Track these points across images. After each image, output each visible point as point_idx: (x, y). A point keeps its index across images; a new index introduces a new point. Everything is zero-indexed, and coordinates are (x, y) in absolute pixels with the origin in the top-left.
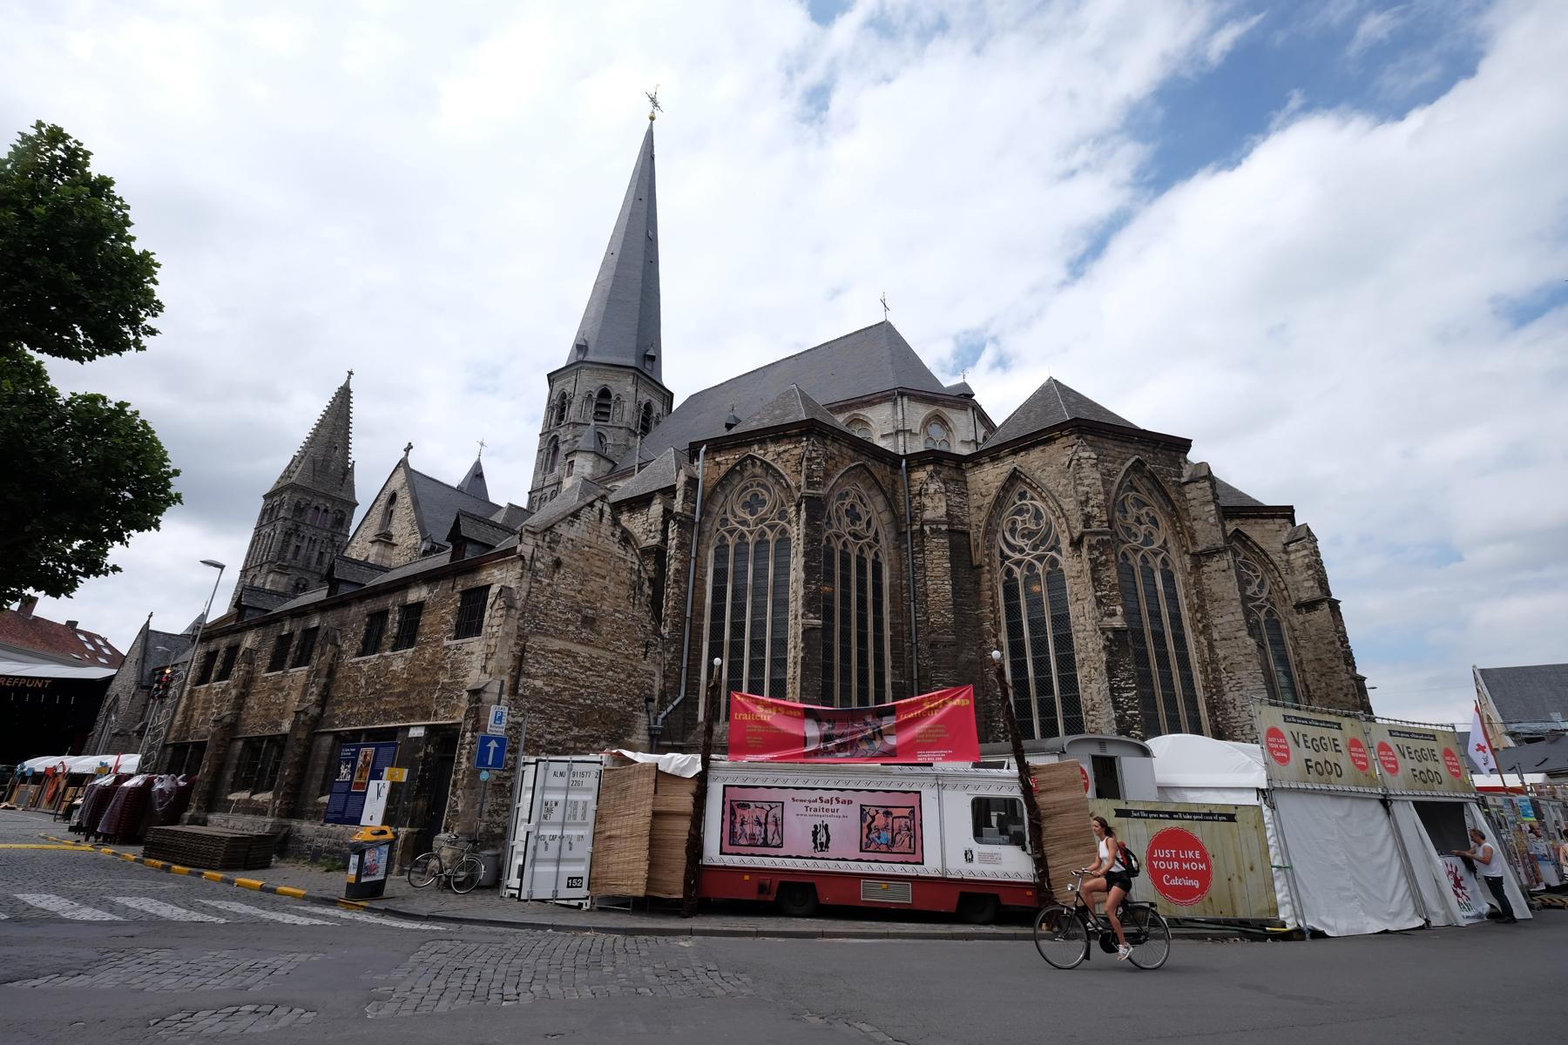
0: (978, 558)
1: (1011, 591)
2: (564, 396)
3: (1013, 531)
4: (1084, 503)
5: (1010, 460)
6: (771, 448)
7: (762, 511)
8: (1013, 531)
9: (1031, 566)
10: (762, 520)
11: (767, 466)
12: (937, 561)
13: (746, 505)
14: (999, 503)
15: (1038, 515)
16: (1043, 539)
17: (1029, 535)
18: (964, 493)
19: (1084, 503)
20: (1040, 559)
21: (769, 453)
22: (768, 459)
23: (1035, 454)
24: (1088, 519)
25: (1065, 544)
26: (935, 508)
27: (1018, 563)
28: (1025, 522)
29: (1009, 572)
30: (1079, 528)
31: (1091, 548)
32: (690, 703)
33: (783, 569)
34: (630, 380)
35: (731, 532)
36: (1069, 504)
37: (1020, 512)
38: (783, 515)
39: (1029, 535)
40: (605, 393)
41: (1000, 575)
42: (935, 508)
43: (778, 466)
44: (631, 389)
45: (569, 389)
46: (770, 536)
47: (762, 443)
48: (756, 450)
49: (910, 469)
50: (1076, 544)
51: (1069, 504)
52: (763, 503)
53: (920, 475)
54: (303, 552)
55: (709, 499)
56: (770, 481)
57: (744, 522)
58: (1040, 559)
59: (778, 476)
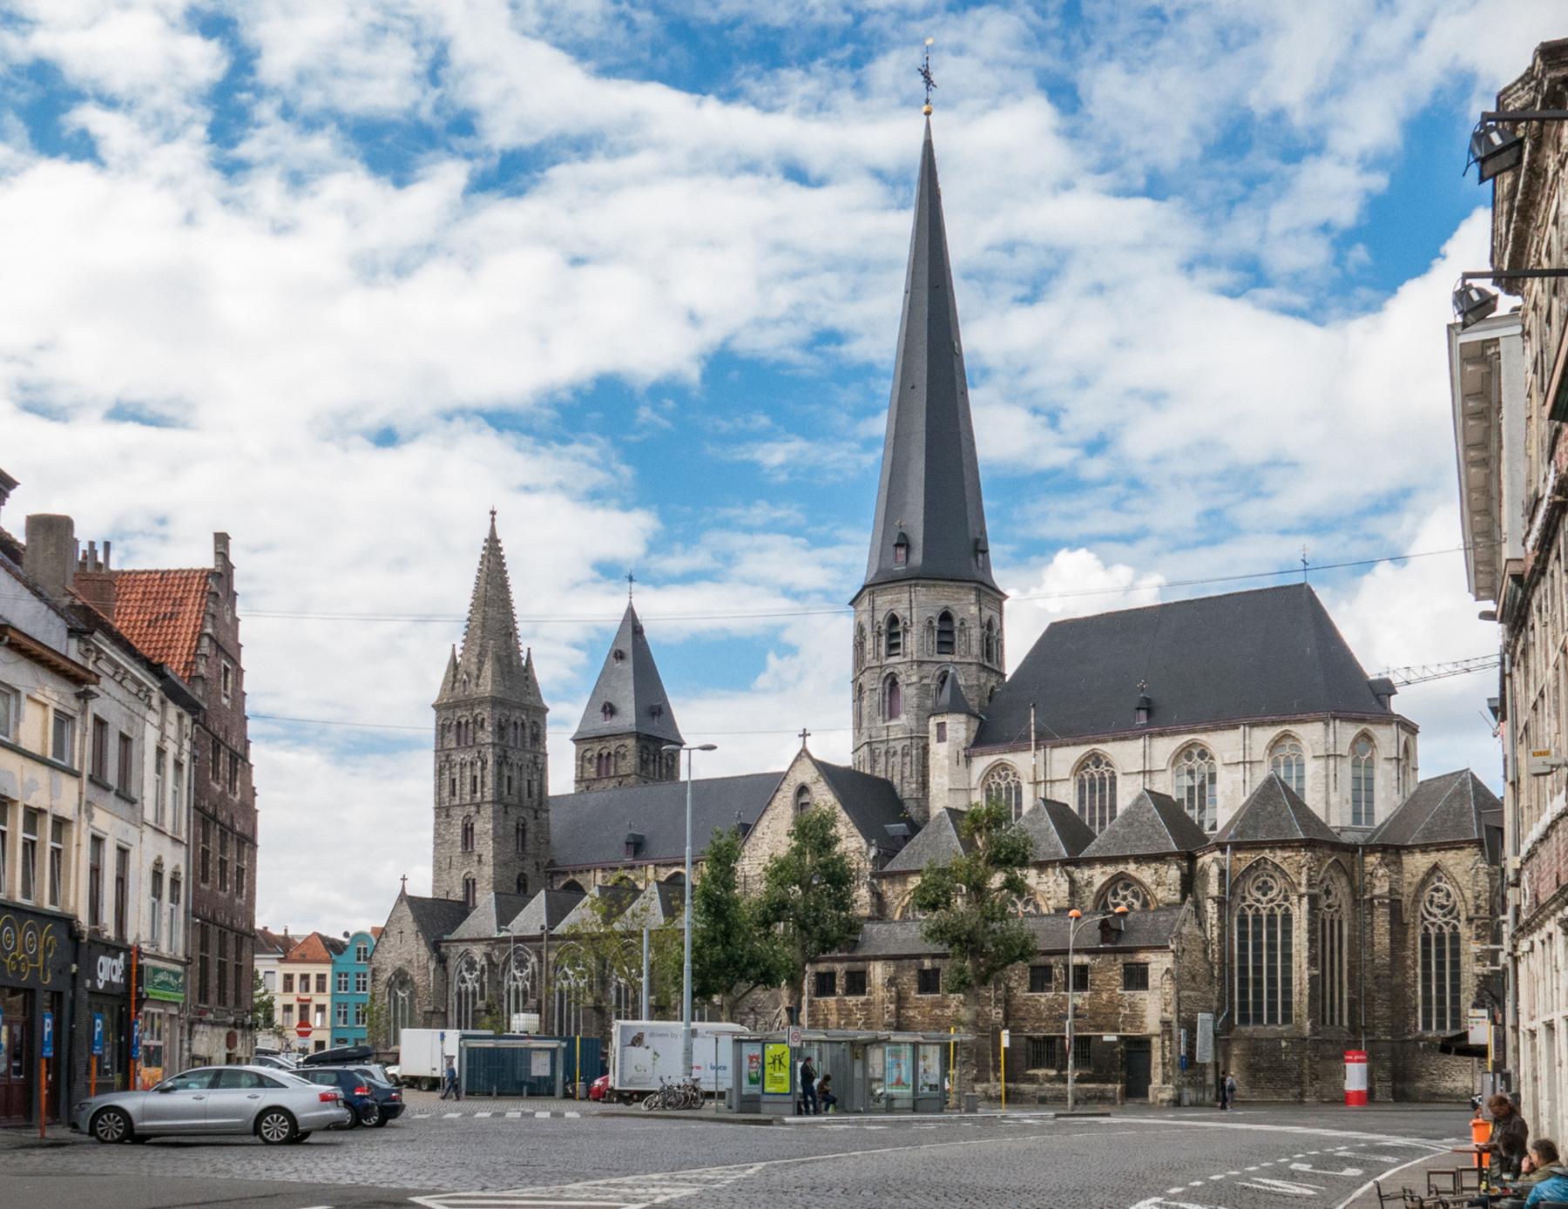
0: (1407, 918)
1: (1426, 941)
2: (893, 620)
3: (1431, 902)
4: (1477, 898)
5: (1434, 854)
6: (1279, 853)
7: (1271, 895)
8: (1431, 902)
9: (1440, 928)
10: (1272, 900)
11: (1276, 867)
12: (1382, 921)
13: (1258, 888)
14: (1424, 883)
15: (1448, 895)
16: (1451, 911)
17: (1442, 907)
18: (1400, 872)
19: (1477, 898)
20: (1447, 923)
21: (1278, 856)
22: (1277, 861)
23: (1451, 854)
24: (1478, 908)
25: (1463, 917)
26: (1382, 888)
27: (1433, 924)
28: (1439, 898)
29: (1426, 929)
30: (1472, 913)
31: (1478, 927)
32: (1230, 1015)
33: (1287, 933)
34: (972, 597)
35: (1250, 907)
36: (1468, 894)
37: (1437, 890)
38: (1286, 899)
39: (1442, 907)
40: (946, 617)
41: (1420, 931)
42: (1382, 888)
43: (1284, 866)
44: (974, 610)
45: (901, 611)
46: (1279, 912)
47: (1272, 849)
48: (1267, 854)
49: (1364, 855)
50: (1470, 920)
51: (1468, 894)
52: (1271, 888)
53: (1373, 860)
54: (515, 784)
55: (1234, 885)
56: (1277, 875)
57: (1258, 901)
58: (1447, 923)
59: (1284, 874)
